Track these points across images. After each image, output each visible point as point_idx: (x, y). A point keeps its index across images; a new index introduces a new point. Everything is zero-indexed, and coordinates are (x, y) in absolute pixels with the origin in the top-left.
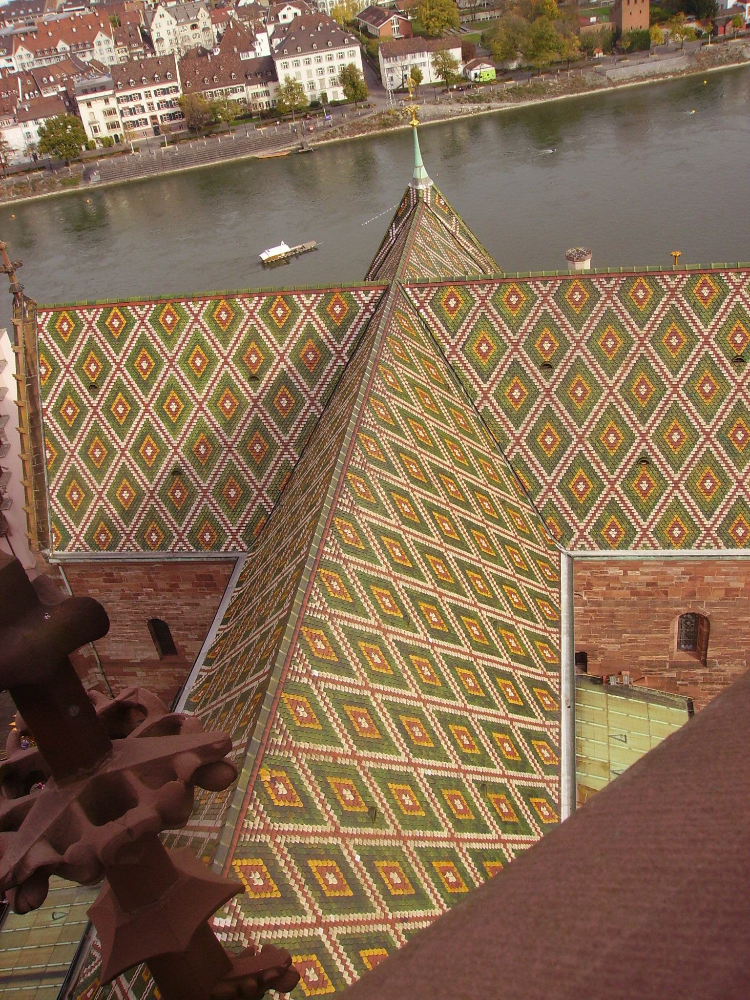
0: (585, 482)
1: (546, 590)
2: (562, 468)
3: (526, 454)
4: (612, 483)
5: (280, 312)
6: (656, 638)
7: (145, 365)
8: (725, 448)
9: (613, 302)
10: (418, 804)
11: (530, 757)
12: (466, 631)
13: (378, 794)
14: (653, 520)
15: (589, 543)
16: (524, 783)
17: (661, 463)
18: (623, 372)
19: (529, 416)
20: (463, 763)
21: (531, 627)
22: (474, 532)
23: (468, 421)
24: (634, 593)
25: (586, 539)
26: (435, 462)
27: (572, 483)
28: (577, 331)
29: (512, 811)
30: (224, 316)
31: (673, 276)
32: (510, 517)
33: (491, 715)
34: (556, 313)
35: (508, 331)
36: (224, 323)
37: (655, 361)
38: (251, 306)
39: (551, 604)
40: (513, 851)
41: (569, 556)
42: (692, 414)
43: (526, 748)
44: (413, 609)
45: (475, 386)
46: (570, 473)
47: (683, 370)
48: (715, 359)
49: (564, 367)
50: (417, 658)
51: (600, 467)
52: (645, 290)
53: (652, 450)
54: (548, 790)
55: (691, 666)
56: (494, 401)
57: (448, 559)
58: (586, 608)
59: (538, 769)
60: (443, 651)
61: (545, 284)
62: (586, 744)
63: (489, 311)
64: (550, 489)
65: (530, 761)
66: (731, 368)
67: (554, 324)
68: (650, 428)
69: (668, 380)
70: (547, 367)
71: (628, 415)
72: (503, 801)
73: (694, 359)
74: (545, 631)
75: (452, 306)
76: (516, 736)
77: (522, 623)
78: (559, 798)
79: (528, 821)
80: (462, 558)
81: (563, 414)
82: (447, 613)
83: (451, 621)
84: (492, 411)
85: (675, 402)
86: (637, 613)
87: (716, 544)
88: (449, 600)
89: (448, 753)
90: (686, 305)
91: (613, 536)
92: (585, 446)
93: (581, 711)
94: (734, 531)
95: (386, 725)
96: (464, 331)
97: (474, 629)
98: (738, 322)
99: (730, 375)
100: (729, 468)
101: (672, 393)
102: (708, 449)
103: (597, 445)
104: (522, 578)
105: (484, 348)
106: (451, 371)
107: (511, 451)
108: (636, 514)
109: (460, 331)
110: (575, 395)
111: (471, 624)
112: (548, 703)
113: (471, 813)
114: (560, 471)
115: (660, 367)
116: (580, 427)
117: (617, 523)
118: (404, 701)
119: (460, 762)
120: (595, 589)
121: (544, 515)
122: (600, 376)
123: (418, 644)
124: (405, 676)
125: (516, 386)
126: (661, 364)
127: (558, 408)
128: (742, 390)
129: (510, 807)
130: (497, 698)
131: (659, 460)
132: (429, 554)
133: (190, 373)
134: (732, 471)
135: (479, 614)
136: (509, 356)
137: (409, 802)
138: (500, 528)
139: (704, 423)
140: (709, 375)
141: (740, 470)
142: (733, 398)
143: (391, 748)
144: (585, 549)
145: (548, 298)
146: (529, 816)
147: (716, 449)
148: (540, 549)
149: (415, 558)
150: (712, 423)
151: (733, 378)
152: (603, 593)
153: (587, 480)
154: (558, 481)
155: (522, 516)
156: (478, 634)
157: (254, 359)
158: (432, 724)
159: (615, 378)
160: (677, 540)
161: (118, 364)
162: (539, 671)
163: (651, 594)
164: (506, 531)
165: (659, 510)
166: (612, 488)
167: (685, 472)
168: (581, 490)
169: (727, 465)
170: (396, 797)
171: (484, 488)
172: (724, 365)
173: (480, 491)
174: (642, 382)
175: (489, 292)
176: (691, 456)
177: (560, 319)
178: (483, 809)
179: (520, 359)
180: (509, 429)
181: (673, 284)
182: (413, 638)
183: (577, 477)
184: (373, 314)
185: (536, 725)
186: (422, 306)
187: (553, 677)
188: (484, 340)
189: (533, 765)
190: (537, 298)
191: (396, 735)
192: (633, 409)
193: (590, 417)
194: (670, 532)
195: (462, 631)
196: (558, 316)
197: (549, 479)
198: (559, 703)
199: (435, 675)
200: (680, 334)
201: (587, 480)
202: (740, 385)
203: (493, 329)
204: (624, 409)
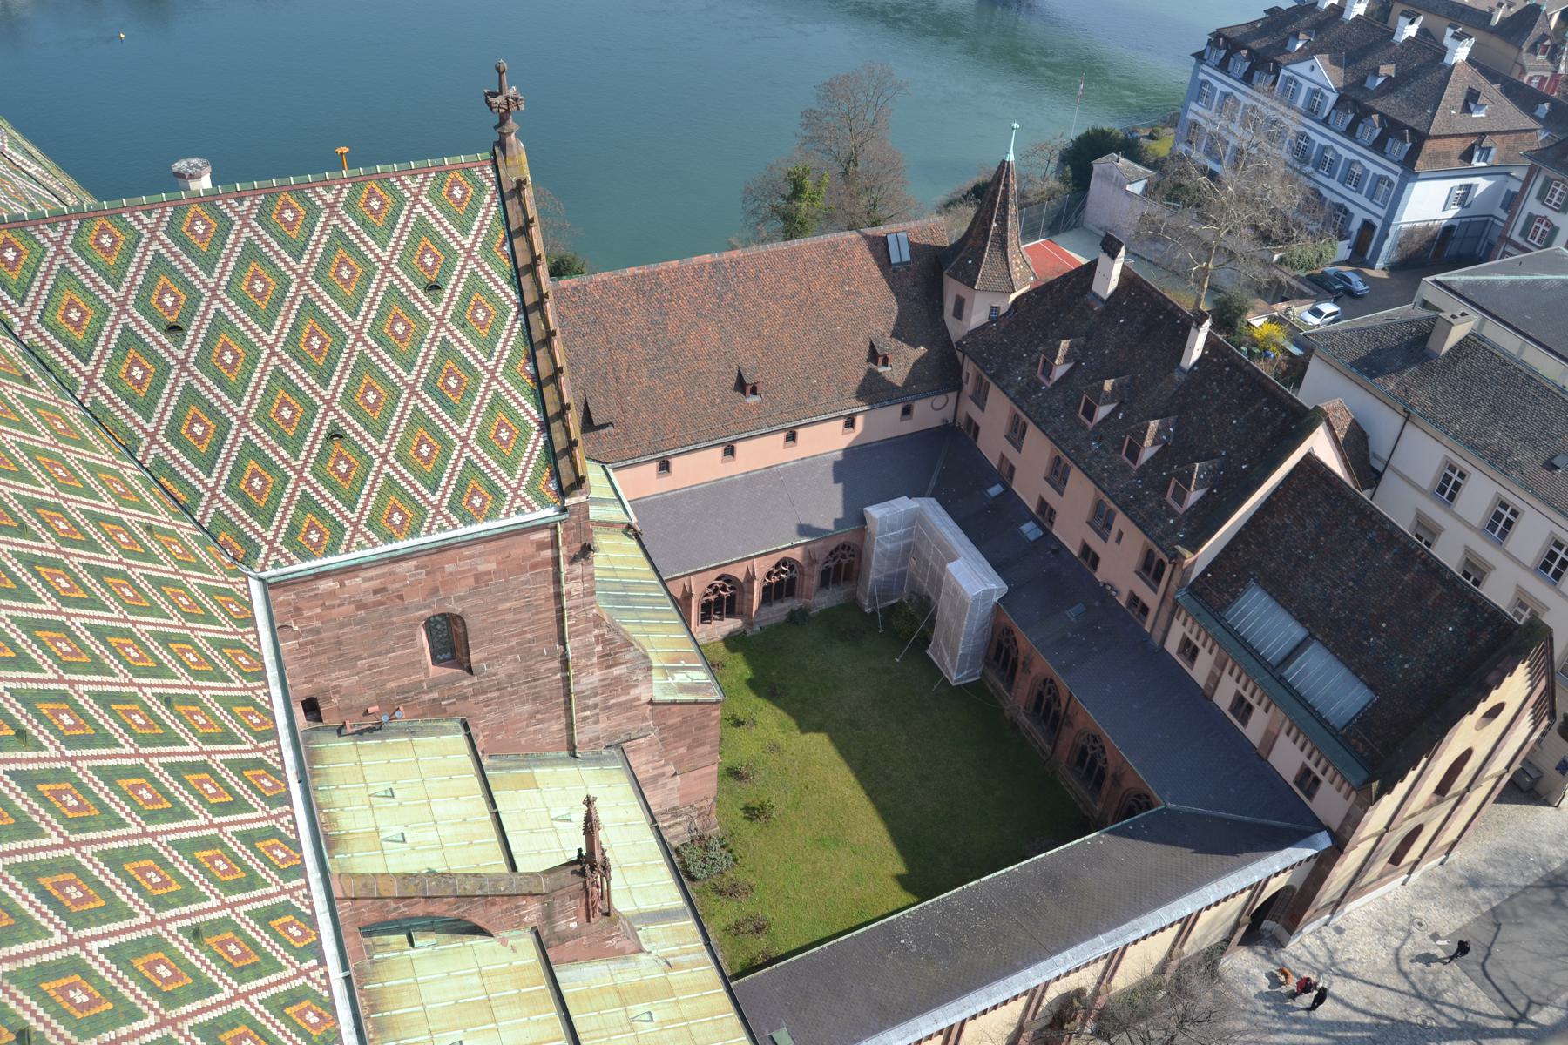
0: (262, 478)
1: (236, 633)
2: (225, 464)
3: (169, 453)
4: (299, 472)
6: (400, 656)
8: (437, 401)
9: (252, 230)
10: (98, 995)
11: (258, 866)
12: (123, 725)
13: (26, 1008)
14: (364, 509)
15: (284, 556)
16: (257, 905)
17: (359, 434)
18: (284, 322)
19: (162, 401)
20: (157, 911)
21: (224, 689)
22: (109, 580)
23: (70, 423)
24: (360, 606)
25: (279, 552)
26: (26, 493)
27: (244, 482)
28: (209, 276)
29: (248, 949)
31: (328, 187)
32: (162, 545)
33: (184, 830)
34: (173, 253)
35: (107, 287)
37: (325, 303)
39: (248, 650)
40: (260, 1002)
41: (260, 579)
42: (387, 365)
43: (249, 857)
44: (30, 716)
45: (72, 371)
46: (238, 470)
47: (364, 309)
48: (403, 290)
49: (199, 327)
50: (52, 787)
51: (277, 454)
52: (293, 209)
53: (343, 419)
54: (293, 901)
55: (451, 681)
56: (106, 388)
57: (73, 629)
58: (301, 640)
59: (273, 879)
60: (90, 763)
61: (149, 215)
62: (342, 814)
63: (72, 261)
64: (214, 495)
65: (259, 872)
66: (425, 299)
67: (174, 269)
68: (335, 390)
69: (347, 324)
70: (174, 329)
71: (303, 379)
72: (230, 941)
73: (375, 294)
74: (245, 689)
75: (12, 259)
76: (231, 845)
77: (209, 688)
78: (311, 906)
79: (274, 954)
80: (96, 622)
81: (211, 392)
82: (87, 707)
83: (96, 717)
84: (105, 402)
85: (361, 352)
86: (370, 631)
87: (450, 522)
88: (86, 688)
89: (131, 905)
90: (353, 224)
91: (315, 540)
92: (251, 429)
93: (326, 775)
94: (469, 503)
95: (19, 900)
96: (38, 294)
97: (136, 717)
98: (424, 238)
99: (426, 307)
100: (448, 425)
101: (356, 341)
102: (416, 406)
103: (268, 424)
104: (197, 625)
105: (74, 315)
106: (30, 355)
107: (146, 454)
108: (339, 505)
109: (32, 294)
110: (223, 363)
111: (128, 713)
112: (269, 784)
113: (185, 976)
114: (223, 468)
115: (332, 310)
116: (239, 404)
117: (317, 523)
118: (42, 855)
119: (152, 911)
120: (307, 614)
121: (213, 532)
122: (254, 332)
123: (47, 765)
124: (36, 819)
125: (135, 362)
126: (334, 305)
127: (203, 384)
128: (444, 325)
129: (242, 945)
130: (191, 803)
131: (355, 430)
132: (41, 629)
134: (451, 429)
135: (140, 694)
136: (116, 322)
137: (81, 998)
138: (149, 565)
139: (404, 374)
140: (400, 311)
141: (461, 426)
142: (435, 336)
143: (36, 931)
144: (281, 566)
145: (158, 233)
146: (273, 947)
147: (427, 404)
148: (217, 580)
149: (18, 641)
150: (414, 373)
151: (430, 311)
152: (318, 617)
153: (264, 473)
154: (223, 483)
155: (181, 541)
156: (143, 722)
158: (96, 872)
159: (274, 332)
160: (399, 528)
162: (248, 746)
163: (383, 604)
164: (159, 567)
165: (369, 495)
166: (301, 478)
167: (392, 441)
168: (258, 488)
169: (444, 422)
170: (59, 999)
171: (114, 514)
172: (416, 296)
173: (108, 519)
174: (313, 332)
175: (65, 233)
176: (395, 418)
177: (181, 262)
178: (203, 963)
179: (133, 324)
180: (137, 424)
181: (330, 197)
182: (39, 760)
183: (248, 472)
185: (258, 820)
187: (269, 748)
188: (71, 304)
189: (264, 876)
190: (141, 236)
191: (38, 909)
192: (307, 369)
193: (250, 389)
194: (389, 520)
195: (116, 726)
196: (177, 258)
197: (210, 482)
198: (285, 780)
199: (86, 802)
200: (352, 263)
201: (264, 473)
202: (440, 319)
203: (83, 286)
204: (296, 373)
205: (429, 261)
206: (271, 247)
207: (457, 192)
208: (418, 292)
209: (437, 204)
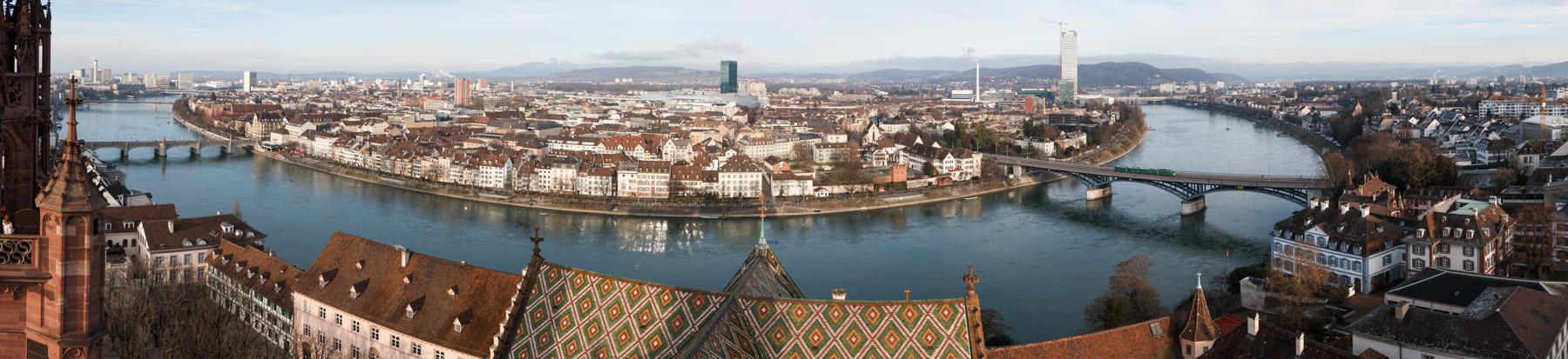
5: (666, 298)
7: (586, 306)
30: (635, 293)
35: (794, 329)
36: (634, 296)
38: (652, 291)
45: (770, 355)
63: (784, 316)
133: (608, 316)
157: (645, 318)
161: (572, 301)
184: (717, 309)
186: (746, 309)
188: (779, 331)
205: (929, 338)
206: (863, 326)
207: (946, 313)
208: (923, 350)
209: (936, 316)
